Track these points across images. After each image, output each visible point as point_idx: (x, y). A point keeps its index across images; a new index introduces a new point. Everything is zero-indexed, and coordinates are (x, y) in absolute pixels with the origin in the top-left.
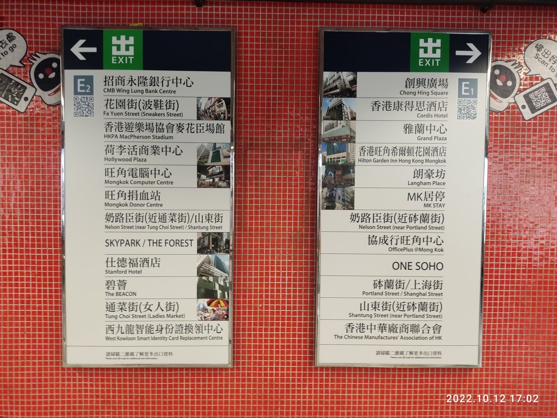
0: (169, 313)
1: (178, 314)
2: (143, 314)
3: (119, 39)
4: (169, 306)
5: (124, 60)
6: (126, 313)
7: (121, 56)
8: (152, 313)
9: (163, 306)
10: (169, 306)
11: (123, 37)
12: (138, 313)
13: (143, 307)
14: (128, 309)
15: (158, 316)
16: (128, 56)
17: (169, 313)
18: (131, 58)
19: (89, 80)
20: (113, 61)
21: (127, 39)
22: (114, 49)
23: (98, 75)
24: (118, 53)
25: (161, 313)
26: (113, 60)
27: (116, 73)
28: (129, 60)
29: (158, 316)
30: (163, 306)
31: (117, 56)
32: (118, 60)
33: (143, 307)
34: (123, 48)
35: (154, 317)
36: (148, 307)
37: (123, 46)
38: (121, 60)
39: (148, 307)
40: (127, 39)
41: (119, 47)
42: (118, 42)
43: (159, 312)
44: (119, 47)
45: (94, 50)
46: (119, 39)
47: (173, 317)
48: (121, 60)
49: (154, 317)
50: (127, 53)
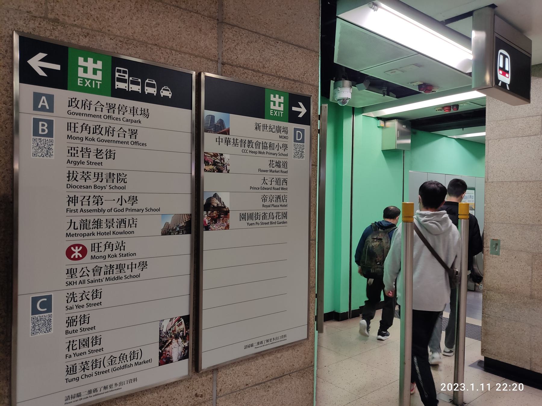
3: (86, 60)
5: (91, 83)
11: (90, 60)
16: (95, 80)
18: (99, 83)
22: (81, 70)
23: (61, 96)
26: (79, 82)
27: (81, 96)
28: (96, 84)
31: (84, 78)
32: (84, 83)
34: (90, 71)
37: (89, 69)
38: (88, 83)
41: (85, 70)
44: (85, 70)
45: (57, 67)
46: (86, 60)
48: (88, 83)
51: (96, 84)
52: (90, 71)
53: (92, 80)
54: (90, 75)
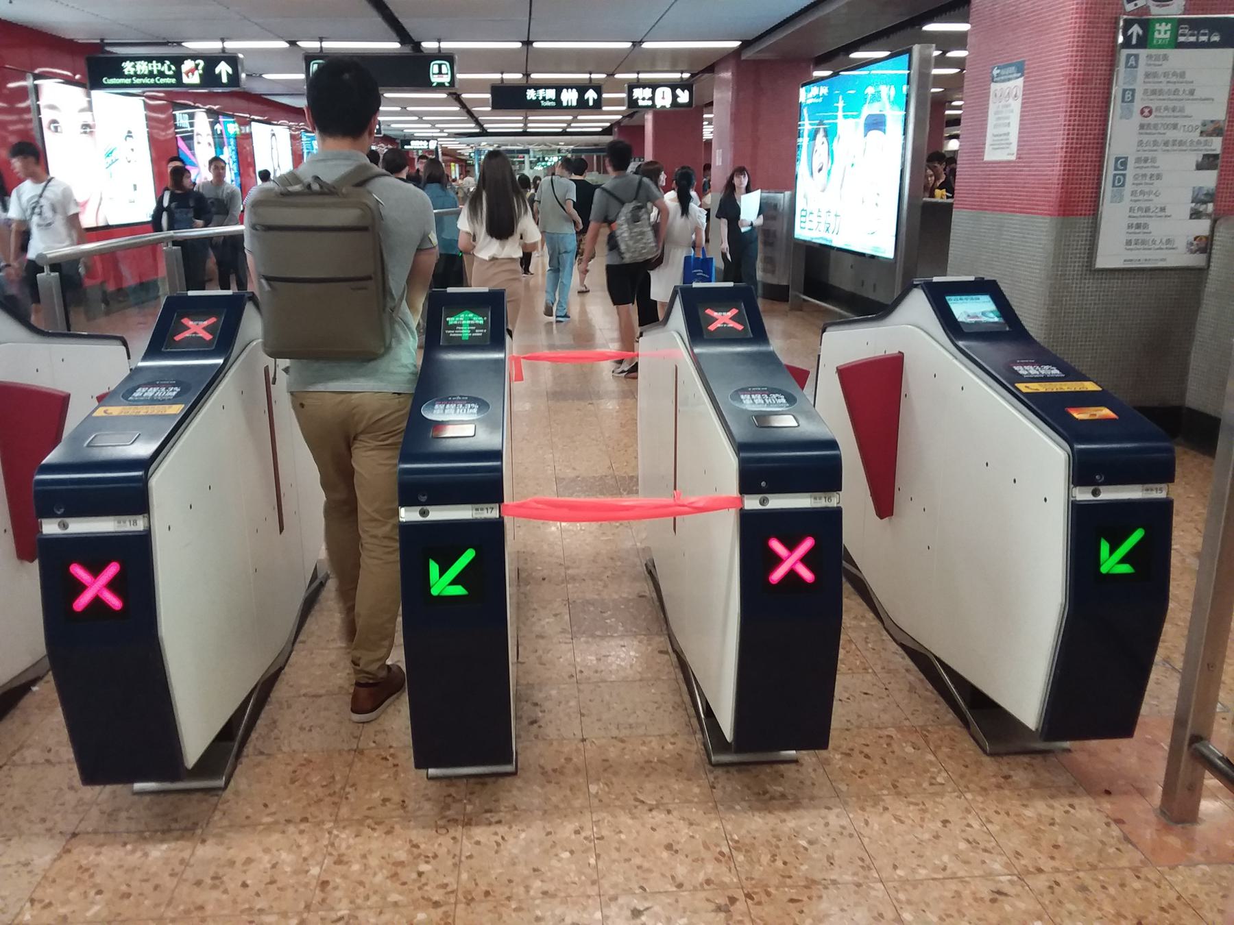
19: (1137, 56)
54: (1162, 36)
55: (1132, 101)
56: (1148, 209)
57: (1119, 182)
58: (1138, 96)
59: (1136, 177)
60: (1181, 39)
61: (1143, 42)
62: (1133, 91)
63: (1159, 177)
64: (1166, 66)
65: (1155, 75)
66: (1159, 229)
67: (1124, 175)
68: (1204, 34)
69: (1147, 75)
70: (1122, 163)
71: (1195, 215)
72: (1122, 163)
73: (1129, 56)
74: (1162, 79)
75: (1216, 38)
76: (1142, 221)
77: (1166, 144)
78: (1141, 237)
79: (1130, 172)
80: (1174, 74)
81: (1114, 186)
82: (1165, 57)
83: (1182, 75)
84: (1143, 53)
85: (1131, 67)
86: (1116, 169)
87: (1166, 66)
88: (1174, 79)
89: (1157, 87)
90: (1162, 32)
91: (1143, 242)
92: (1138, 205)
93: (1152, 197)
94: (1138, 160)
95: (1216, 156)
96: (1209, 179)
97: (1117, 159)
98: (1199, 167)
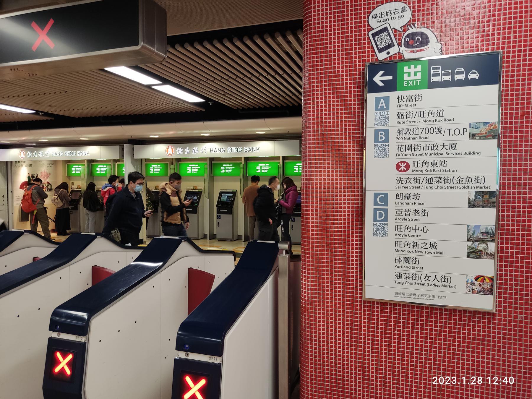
0: (443, 283)
1: (451, 285)
2: (423, 283)
3: (409, 68)
4: (444, 279)
5: (413, 83)
6: (410, 281)
7: (411, 81)
8: (430, 283)
9: (439, 278)
10: (444, 279)
12: (419, 282)
13: (423, 278)
14: (411, 278)
15: (434, 285)
16: (416, 80)
17: (443, 283)
19: (387, 99)
20: (405, 84)
21: (416, 67)
22: (406, 75)
24: (409, 78)
25: (437, 283)
29: (434, 285)
30: (439, 278)
31: (408, 81)
33: (423, 278)
34: (412, 74)
35: (431, 285)
36: (427, 278)
38: (411, 83)
39: (427, 278)
40: (416, 67)
42: (409, 71)
43: (436, 282)
46: (409, 68)
47: (446, 286)
48: (411, 83)
49: (431, 285)
50: (416, 78)
51: (417, 82)
52: (412, 74)
53: (414, 80)
54: (412, 77)
55: (387, 140)
56: (416, 245)
57: (382, 217)
58: (393, 135)
59: (398, 212)
60: (434, 79)
61: (390, 86)
62: (387, 132)
63: (425, 213)
64: (420, 106)
65: (409, 115)
66: (429, 264)
67: (386, 211)
68: (461, 73)
69: (400, 116)
70: (382, 198)
71: (474, 254)
72: (382, 198)
73: (378, 100)
74: (417, 118)
75: (474, 75)
76: (411, 256)
77: (430, 181)
78: (412, 271)
79: (392, 207)
80: (431, 113)
81: (375, 220)
82: (418, 98)
83: (440, 113)
84: (392, 95)
85: (382, 108)
86: (376, 204)
87: (420, 106)
88: (431, 118)
89: (412, 126)
90: (411, 73)
91: (415, 277)
92: (403, 240)
93: (419, 232)
94: (399, 196)
95: (492, 194)
96: (487, 218)
97: (376, 195)
98: (471, 205)
